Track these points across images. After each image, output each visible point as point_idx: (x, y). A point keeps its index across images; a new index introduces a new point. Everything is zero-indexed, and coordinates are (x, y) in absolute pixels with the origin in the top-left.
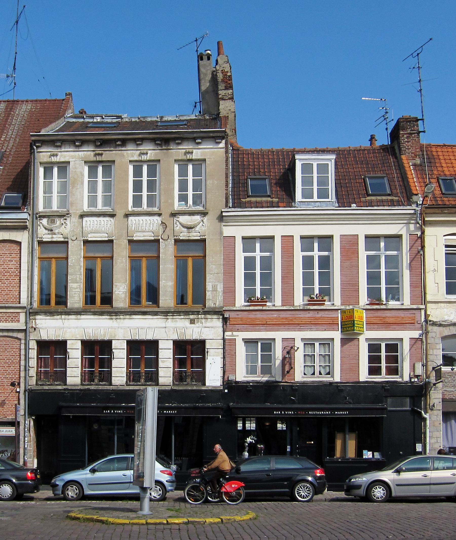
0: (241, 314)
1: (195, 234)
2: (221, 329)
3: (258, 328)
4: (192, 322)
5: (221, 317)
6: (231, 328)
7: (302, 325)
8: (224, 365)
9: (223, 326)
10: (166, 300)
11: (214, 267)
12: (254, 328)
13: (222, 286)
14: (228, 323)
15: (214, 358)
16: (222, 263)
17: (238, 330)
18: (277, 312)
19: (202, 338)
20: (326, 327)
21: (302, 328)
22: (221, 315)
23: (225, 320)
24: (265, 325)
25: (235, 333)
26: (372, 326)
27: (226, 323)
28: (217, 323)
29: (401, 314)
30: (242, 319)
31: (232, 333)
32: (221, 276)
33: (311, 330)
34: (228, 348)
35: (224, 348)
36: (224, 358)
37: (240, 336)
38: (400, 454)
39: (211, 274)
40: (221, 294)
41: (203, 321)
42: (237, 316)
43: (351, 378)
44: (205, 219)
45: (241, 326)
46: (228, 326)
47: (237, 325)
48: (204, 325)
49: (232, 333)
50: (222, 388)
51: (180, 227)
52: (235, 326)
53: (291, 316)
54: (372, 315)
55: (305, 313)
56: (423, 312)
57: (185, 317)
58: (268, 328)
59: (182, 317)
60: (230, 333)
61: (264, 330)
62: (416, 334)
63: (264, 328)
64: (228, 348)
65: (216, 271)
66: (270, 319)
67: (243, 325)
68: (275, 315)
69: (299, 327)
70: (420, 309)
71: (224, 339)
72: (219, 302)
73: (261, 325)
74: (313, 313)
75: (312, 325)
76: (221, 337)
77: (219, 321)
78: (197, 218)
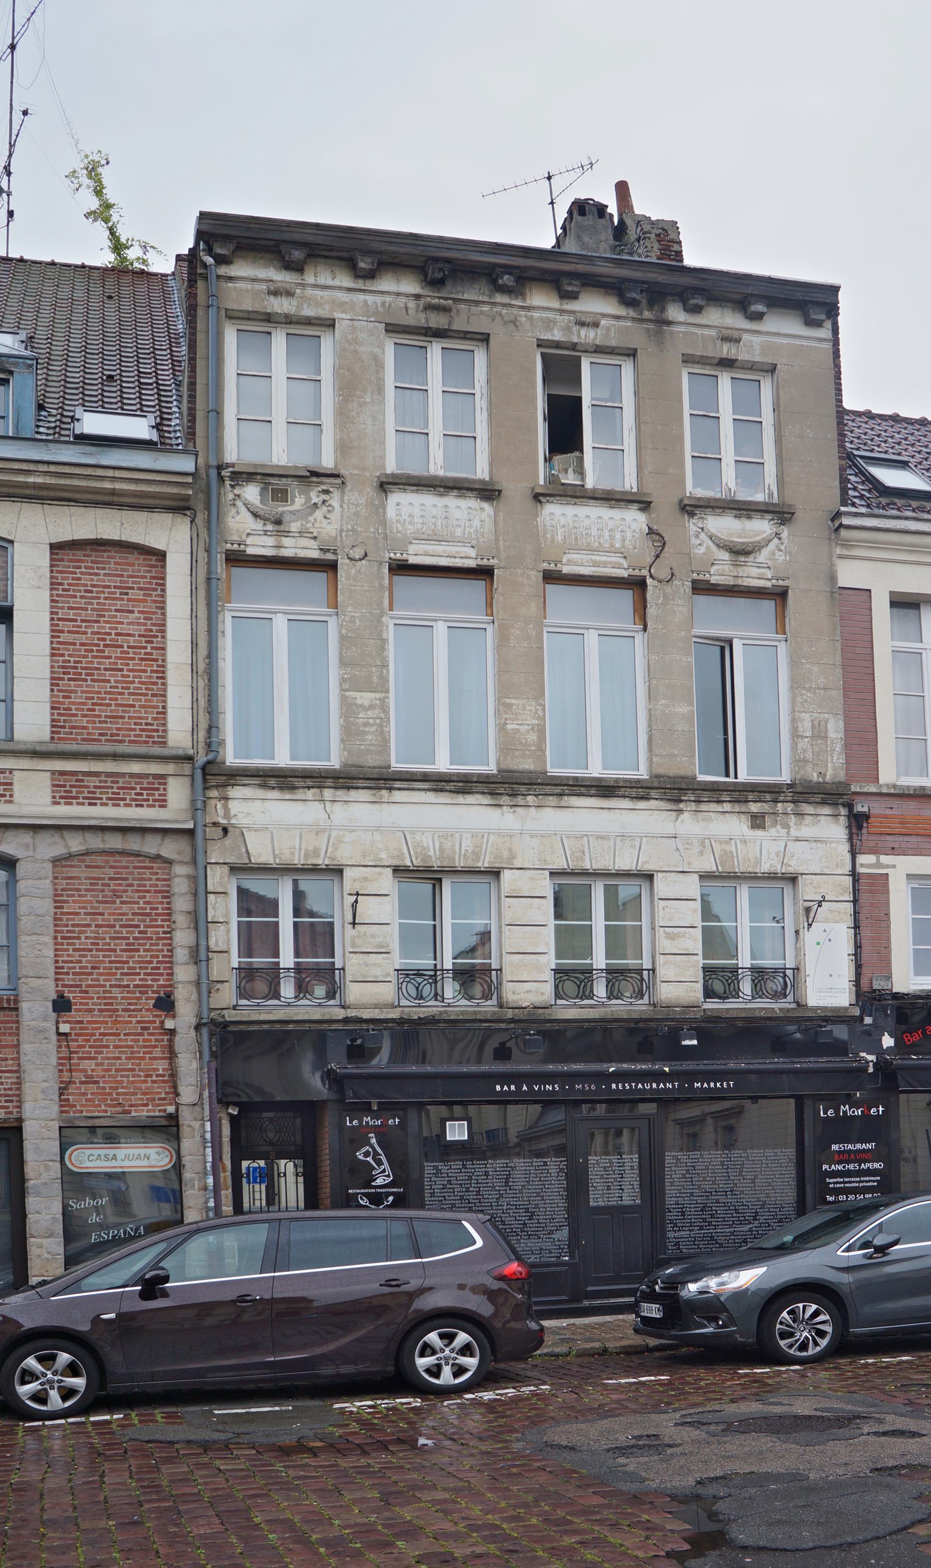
1: (754, 571)
2: (845, 848)
4: (757, 822)
6: (871, 844)
9: (850, 839)
10: (673, 755)
11: (816, 669)
14: (864, 831)
15: (828, 926)
16: (839, 658)
17: (893, 851)
19: (791, 870)
22: (844, 805)
23: (857, 822)
25: (884, 859)
27: (860, 828)
28: (831, 829)
34: (867, 897)
35: (855, 901)
36: (856, 927)
37: (900, 870)
39: (809, 689)
40: (838, 749)
41: (793, 820)
42: (888, 812)
44: (785, 532)
45: (901, 838)
47: (889, 838)
48: (794, 832)
51: (708, 548)
57: (737, 808)
59: (727, 807)
64: (867, 897)
65: (821, 681)
67: (907, 838)
71: (854, 874)
72: (835, 769)
76: (848, 867)
78: (762, 527)
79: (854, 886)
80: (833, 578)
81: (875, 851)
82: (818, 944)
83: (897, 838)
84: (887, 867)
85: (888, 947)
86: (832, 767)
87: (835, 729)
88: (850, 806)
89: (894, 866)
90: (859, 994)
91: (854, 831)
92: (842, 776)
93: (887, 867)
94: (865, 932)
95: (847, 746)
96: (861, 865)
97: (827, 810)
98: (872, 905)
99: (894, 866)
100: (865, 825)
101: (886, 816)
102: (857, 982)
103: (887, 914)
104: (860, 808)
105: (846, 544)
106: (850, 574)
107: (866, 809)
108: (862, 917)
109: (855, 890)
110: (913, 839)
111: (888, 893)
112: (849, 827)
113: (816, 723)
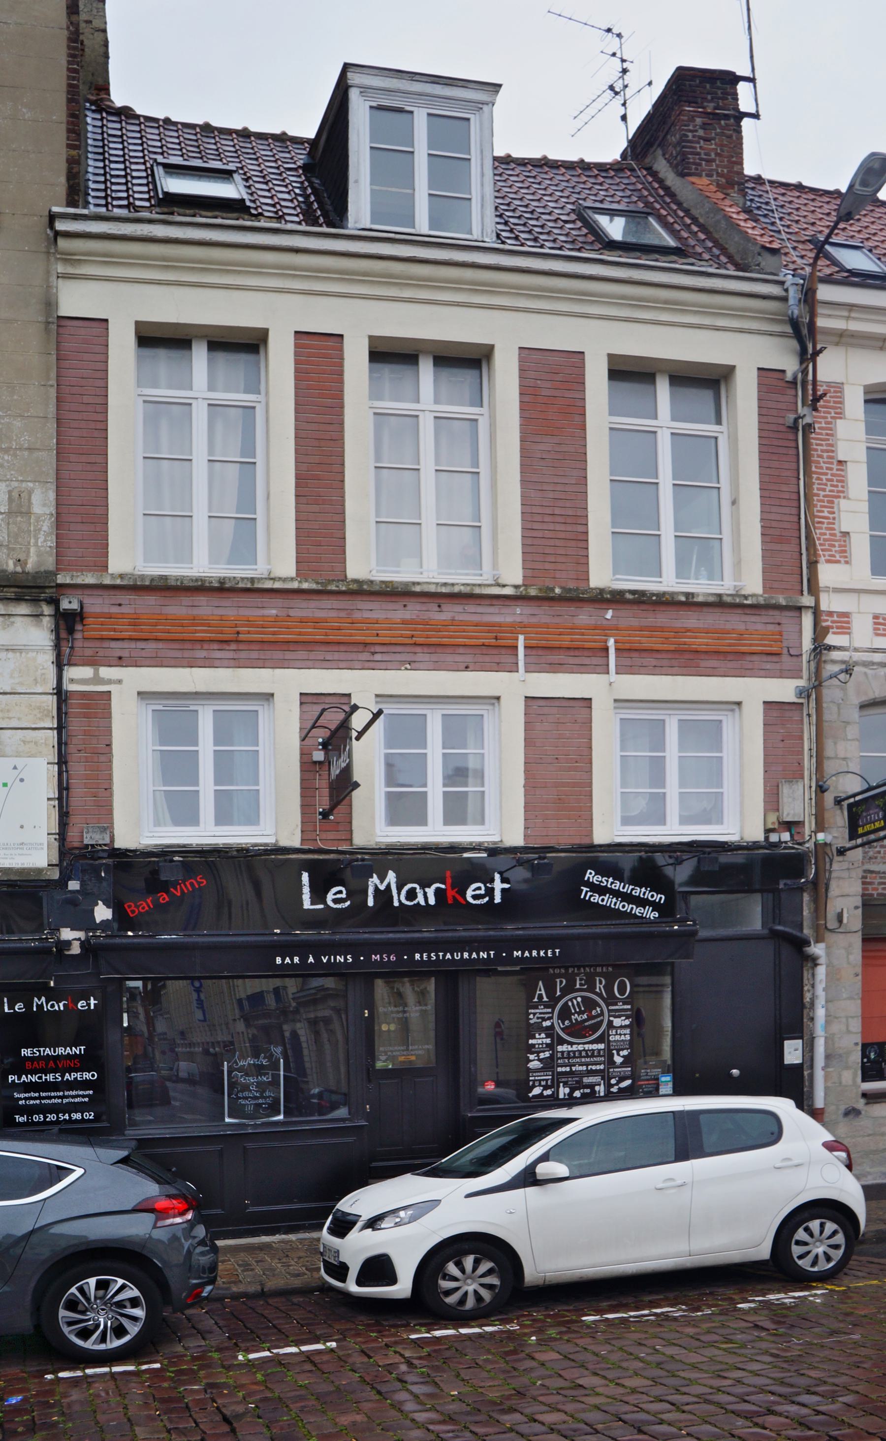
0: (133, 605)
2: (47, 659)
3: (202, 654)
5: (47, 610)
6: (88, 652)
7: (378, 649)
8: (64, 788)
9: (57, 647)
11: (18, 423)
12: (187, 654)
13: (52, 495)
14: (78, 635)
15: (20, 762)
17: (120, 661)
18: (279, 601)
20: (468, 659)
21: (378, 657)
23: (67, 624)
24: (233, 646)
25: (105, 672)
26: (637, 659)
27: (71, 631)
29: (735, 622)
30: (135, 621)
31: (96, 673)
32: (49, 459)
33: (413, 665)
35: (60, 728)
36: (62, 761)
38: (731, 1075)
40: (45, 528)
42: (115, 610)
43: (561, 834)
45: (133, 645)
46: (78, 644)
47: (113, 644)
49: (96, 673)
50: (55, 875)
52: (106, 644)
53: (333, 614)
54: (635, 622)
55: (391, 606)
56: (807, 620)
58: (243, 655)
60: (86, 672)
61: (226, 662)
62: (785, 690)
63: (230, 655)
65: (25, 440)
66: (249, 622)
67: (141, 645)
68: (272, 610)
69: (365, 656)
70: (799, 609)
71: (60, 692)
72: (39, 554)
73: (215, 646)
74: (419, 607)
75: (418, 649)
76: (52, 683)
77: (39, 624)
79: (59, 709)
80: (50, 304)
81: (93, 662)
82: (5, 785)
83: (126, 644)
84: (109, 682)
85: (109, 789)
86: (37, 553)
87: (43, 502)
88: (54, 602)
89: (120, 682)
90: (63, 852)
91: (63, 634)
92: (50, 563)
93: (109, 682)
94: (76, 768)
95: (60, 522)
96: (72, 681)
97: (23, 609)
98: (86, 733)
99: (120, 682)
100: (79, 627)
101: (110, 616)
102: (62, 835)
103: (109, 745)
104: (65, 605)
105: (69, 258)
106: (76, 300)
107: (75, 606)
108: (72, 748)
109: (61, 714)
110: (152, 645)
111: (110, 717)
112: (57, 630)
113: (15, 495)
